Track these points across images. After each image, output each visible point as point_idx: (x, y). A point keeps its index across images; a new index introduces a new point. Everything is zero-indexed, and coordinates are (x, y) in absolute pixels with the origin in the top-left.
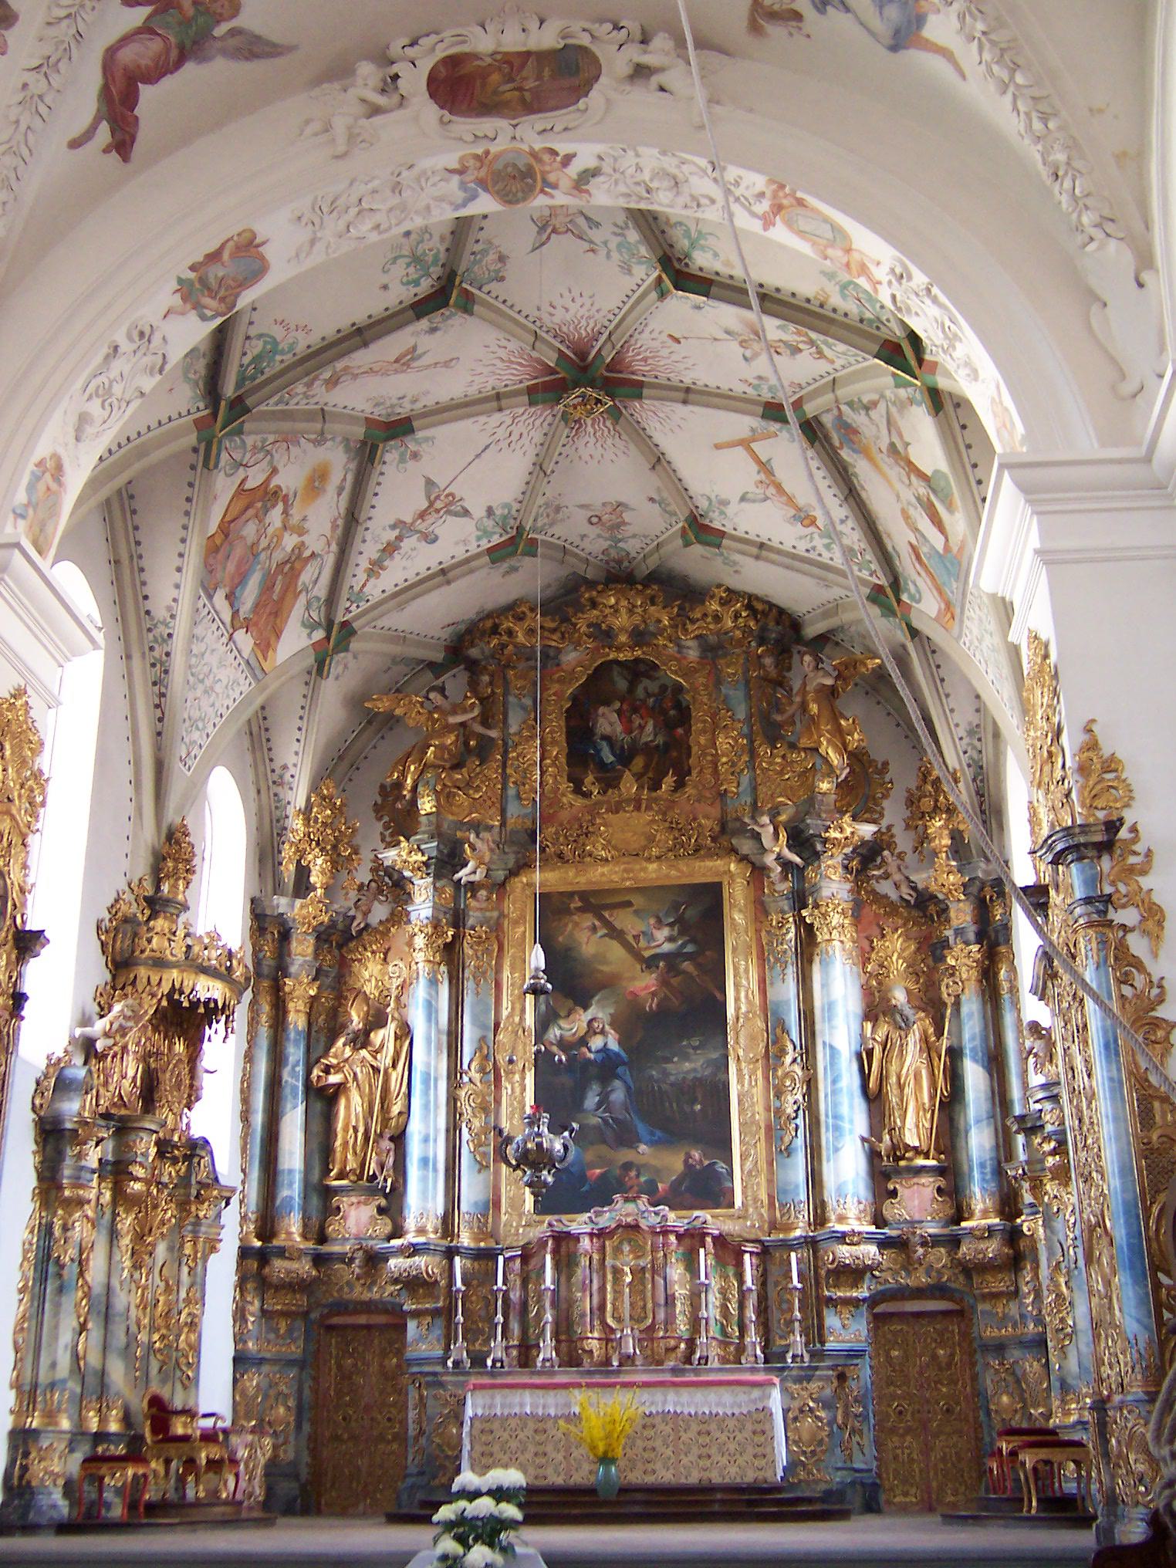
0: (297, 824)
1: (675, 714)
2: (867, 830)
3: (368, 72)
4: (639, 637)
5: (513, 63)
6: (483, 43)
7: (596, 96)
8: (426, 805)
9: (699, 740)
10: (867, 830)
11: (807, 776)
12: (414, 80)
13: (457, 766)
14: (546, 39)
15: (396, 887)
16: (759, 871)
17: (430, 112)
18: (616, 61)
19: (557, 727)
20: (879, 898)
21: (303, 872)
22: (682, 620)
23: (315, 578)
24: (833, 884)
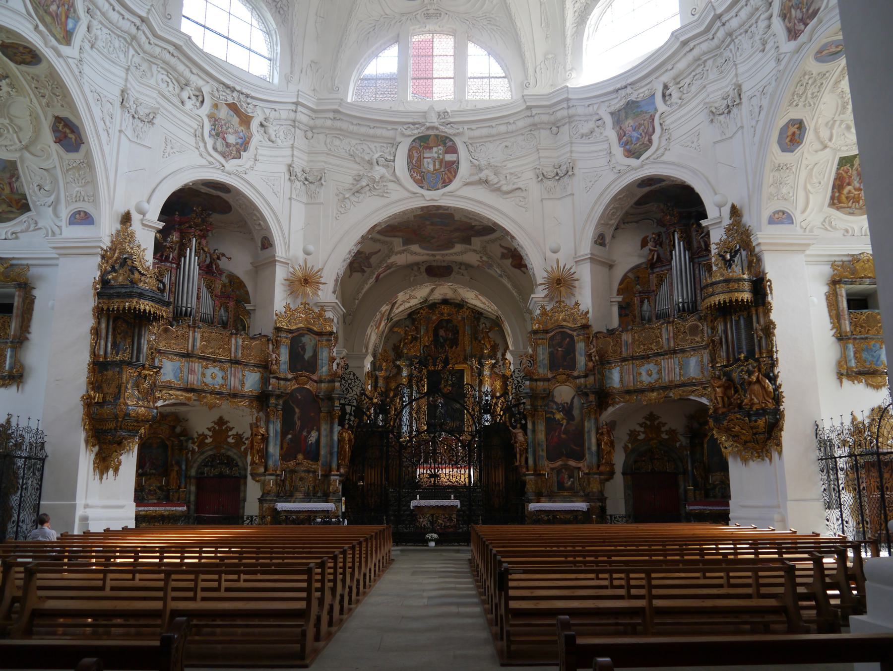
0: (379, 355)
1: (455, 331)
2: (493, 361)
3: (416, 268)
4: (449, 315)
5: (439, 267)
6: (435, 264)
7: (452, 276)
8: (405, 351)
9: (460, 338)
10: (493, 361)
11: (482, 349)
12: (423, 269)
13: (411, 343)
14: (445, 264)
15: (399, 369)
16: (472, 368)
17: (425, 275)
18: (456, 269)
19: (431, 333)
20: (496, 373)
21: (381, 365)
22: (458, 312)
23: (387, 313)
24: (487, 372)
